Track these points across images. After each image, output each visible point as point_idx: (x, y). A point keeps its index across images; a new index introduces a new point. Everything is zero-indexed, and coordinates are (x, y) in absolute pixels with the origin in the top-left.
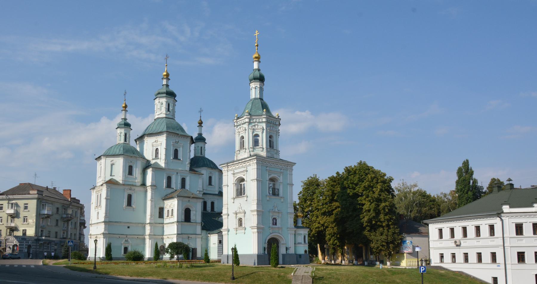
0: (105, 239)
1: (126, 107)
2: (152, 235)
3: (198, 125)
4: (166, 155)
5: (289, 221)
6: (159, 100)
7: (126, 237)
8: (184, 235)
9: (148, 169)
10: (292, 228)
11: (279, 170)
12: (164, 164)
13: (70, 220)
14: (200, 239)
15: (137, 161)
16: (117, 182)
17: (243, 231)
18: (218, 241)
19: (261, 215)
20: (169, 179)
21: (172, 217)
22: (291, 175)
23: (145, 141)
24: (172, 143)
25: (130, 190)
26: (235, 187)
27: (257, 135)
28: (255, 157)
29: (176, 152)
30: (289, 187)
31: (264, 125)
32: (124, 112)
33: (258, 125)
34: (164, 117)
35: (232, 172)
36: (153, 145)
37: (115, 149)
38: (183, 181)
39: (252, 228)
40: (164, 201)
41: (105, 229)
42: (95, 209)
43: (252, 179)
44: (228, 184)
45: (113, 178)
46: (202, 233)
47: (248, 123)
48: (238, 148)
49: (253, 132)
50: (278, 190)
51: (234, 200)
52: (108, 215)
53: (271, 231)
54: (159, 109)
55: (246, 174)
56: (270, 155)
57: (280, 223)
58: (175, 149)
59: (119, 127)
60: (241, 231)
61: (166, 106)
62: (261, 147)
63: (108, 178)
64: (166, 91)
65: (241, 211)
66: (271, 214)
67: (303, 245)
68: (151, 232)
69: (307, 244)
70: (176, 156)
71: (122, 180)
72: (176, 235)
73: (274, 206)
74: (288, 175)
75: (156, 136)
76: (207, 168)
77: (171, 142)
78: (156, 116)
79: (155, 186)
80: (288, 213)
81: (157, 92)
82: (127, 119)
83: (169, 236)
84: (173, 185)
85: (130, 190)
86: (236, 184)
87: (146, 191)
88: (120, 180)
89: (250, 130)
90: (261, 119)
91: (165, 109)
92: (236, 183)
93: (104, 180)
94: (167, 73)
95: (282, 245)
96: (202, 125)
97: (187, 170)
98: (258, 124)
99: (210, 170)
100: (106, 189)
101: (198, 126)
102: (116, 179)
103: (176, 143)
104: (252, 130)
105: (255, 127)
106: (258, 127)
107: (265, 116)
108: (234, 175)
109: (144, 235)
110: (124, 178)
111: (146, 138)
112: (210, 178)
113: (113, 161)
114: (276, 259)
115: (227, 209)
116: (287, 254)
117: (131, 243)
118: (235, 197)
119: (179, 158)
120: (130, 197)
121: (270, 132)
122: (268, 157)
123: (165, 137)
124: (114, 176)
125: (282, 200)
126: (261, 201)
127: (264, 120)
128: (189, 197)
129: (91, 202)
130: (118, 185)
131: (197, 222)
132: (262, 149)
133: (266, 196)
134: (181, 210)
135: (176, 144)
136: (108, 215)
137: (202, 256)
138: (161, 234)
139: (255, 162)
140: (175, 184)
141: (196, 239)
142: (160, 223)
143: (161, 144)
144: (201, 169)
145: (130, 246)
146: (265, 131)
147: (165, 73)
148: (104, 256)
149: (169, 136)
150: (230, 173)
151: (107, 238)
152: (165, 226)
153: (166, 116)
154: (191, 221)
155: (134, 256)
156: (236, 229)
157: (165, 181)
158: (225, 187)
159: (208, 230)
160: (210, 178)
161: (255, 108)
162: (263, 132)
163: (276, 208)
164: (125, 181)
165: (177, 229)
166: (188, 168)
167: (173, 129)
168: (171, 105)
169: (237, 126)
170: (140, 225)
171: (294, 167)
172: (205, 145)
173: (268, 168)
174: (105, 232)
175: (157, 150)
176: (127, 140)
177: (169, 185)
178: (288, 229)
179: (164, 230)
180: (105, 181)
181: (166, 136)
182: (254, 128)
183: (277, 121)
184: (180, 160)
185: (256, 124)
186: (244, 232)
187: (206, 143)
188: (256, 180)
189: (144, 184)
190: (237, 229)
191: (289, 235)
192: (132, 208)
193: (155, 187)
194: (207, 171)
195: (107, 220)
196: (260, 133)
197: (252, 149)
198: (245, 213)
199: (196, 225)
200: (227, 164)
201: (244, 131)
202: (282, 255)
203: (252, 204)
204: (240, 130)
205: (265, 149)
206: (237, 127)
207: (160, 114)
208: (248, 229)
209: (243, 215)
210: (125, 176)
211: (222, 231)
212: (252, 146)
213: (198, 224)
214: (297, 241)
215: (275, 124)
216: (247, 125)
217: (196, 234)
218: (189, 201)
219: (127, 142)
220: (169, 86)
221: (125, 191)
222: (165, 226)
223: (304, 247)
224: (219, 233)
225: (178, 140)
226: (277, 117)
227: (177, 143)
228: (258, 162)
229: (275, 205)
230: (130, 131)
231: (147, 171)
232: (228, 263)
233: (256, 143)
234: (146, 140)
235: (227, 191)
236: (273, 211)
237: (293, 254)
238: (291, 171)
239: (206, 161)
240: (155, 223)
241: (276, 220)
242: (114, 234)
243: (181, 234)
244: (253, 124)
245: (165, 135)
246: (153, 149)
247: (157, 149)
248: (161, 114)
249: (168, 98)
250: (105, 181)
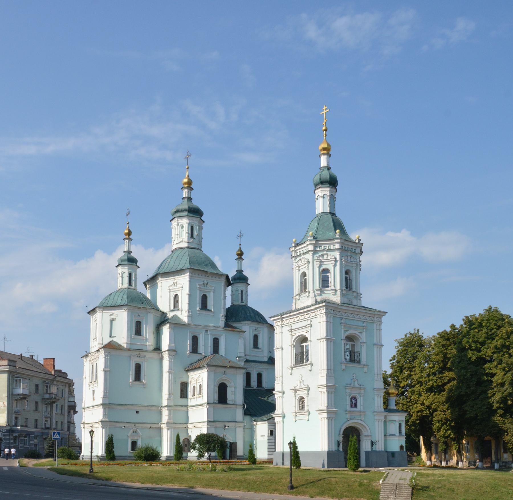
0: (104, 430)
1: (129, 233)
2: (172, 423)
3: (237, 257)
4: (189, 304)
5: (376, 402)
6: (179, 222)
7: (135, 425)
8: (217, 423)
9: (163, 325)
10: (381, 412)
11: (361, 324)
12: (187, 317)
13: (54, 402)
14: (242, 429)
15: (147, 314)
16: (120, 345)
17: (306, 417)
18: (268, 431)
19: (333, 392)
20: (195, 340)
21: (199, 397)
22: (379, 330)
23: (158, 283)
24: (198, 286)
25: (138, 357)
26: (293, 350)
27: (326, 271)
28: (324, 304)
29: (204, 299)
30: (375, 349)
31: (337, 255)
32: (127, 241)
33: (328, 255)
34: (186, 247)
35: (289, 328)
36: (170, 290)
37: (116, 297)
38: (216, 342)
39: (320, 411)
40: (188, 373)
41: (104, 415)
42: (89, 386)
43: (319, 337)
44: (283, 347)
45: (114, 339)
46: (244, 420)
47: (312, 252)
48: (298, 290)
49: (320, 266)
50: (360, 353)
51: (292, 370)
52: (108, 394)
53: (348, 416)
54: (178, 235)
55: (309, 331)
56: (346, 300)
57: (362, 404)
58: (203, 295)
59: (121, 264)
60: (303, 417)
61: (188, 230)
62: (333, 288)
63: (107, 340)
64: (189, 207)
65: (303, 386)
66: (348, 391)
67: (397, 438)
68: (169, 419)
69: (403, 436)
70: (204, 306)
71: (127, 343)
72: (206, 424)
73: (354, 379)
74: (375, 330)
75: (175, 276)
76: (250, 322)
77: (197, 284)
78: (174, 245)
79: (174, 351)
80: (375, 389)
81: (174, 210)
82: (132, 252)
83: (196, 425)
84: (201, 349)
85: (138, 357)
86: (294, 346)
87: (162, 359)
88: (123, 343)
89: (315, 263)
90: (332, 246)
91: (187, 235)
92: (295, 344)
93: (101, 343)
94: (189, 179)
95: (365, 438)
96: (242, 257)
97: (221, 326)
98: (328, 253)
99: (256, 326)
100: (104, 356)
101: (236, 260)
102: (117, 342)
103: (204, 286)
104: (319, 263)
105: (323, 258)
106: (327, 258)
107: (339, 241)
108: (292, 332)
109: (159, 423)
110: (129, 339)
111: (160, 279)
112: (256, 337)
113: (112, 314)
114: (356, 459)
115: (281, 384)
116: (372, 451)
117: (141, 434)
118: (294, 365)
119: (208, 308)
120: (138, 368)
121: (346, 265)
122: (343, 304)
123: (188, 277)
124: (115, 337)
125: (365, 369)
126: (332, 371)
127: (337, 246)
128: (225, 367)
129: (83, 375)
130: (121, 350)
131: (237, 404)
132: (334, 291)
133: (341, 363)
134: (212, 387)
135: (203, 288)
136: (108, 394)
137: (244, 454)
138: (184, 422)
139: (324, 311)
140: (203, 347)
141: (236, 428)
142: (182, 406)
143: (182, 287)
144: (241, 324)
145: (140, 439)
146: (338, 264)
147: (186, 180)
148: (103, 454)
149: (194, 275)
150: (286, 329)
151: (108, 428)
152: (190, 409)
153: (188, 245)
154: (228, 402)
155: (146, 454)
156: (295, 414)
157: (188, 344)
158: (278, 350)
159: (253, 415)
160: (256, 337)
161: (323, 229)
162: (335, 265)
163: (356, 383)
164: (131, 344)
165: (208, 413)
166: (222, 322)
167: (200, 264)
168: (196, 228)
169: (296, 257)
170: (153, 408)
171: (384, 319)
172: (247, 288)
173: (343, 321)
174: (104, 419)
175: (177, 296)
176: (133, 283)
177: (194, 349)
178: (375, 414)
179: (189, 415)
180: (102, 344)
181: (189, 276)
182: (322, 259)
183: (357, 247)
184: (210, 310)
185: (325, 252)
186: (307, 418)
187: (249, 285)
188: (325, 340)
189: (158, 349)
190: (296, 413)
191: (377, 423)
192: (142, 383)
193: (175, 353)
194: (250, 326)
195: (107, 402)
196: (331, 267)
197: (319, 292)
198: (309, 390)
199: (236, 407)
200: (281, 316)
201: (307, 265)
202: (365, 453)
203: (320, 375)
204: (300, 263)
205: (339, 291)
206: (296, 259)
207: (180, 243)
208: (314, 414)
209: (306, 392)
210: (131, 336)
211: (274, 417)
212: (319, 287)
213: (237, 406)
214: (388, 432)
215: (355, 252)
216: (311, 255)
217: (236, 422)
218: (225, 372)
219: (133, 287)
220: (192, 199)
221: (131, 359)
222: (189, 410)
223: (399, 440)
224: (269, 419)
225: (207, 281)
226: (357, 241)
227: (205, 285)
228: (329, 312)
229: (355, 378)
230: (136, 269)
231: (163, 329)
232: (283, 464)
233: (325, 282)
234: (160, 282)
235: (280, 356)
236: (352, 385)
237: (382, 451)
238: (378, 324)
239: (249, 311)
240: (177, 406)
241: (356, 400)
242: (116, 422)
243: (214, 421)
244: (321, 253)
245: (188, 274)
246: (170, 296)
247: (176, 296)
248: (181, 242)
249: (191, 218)
250: (102, 344)
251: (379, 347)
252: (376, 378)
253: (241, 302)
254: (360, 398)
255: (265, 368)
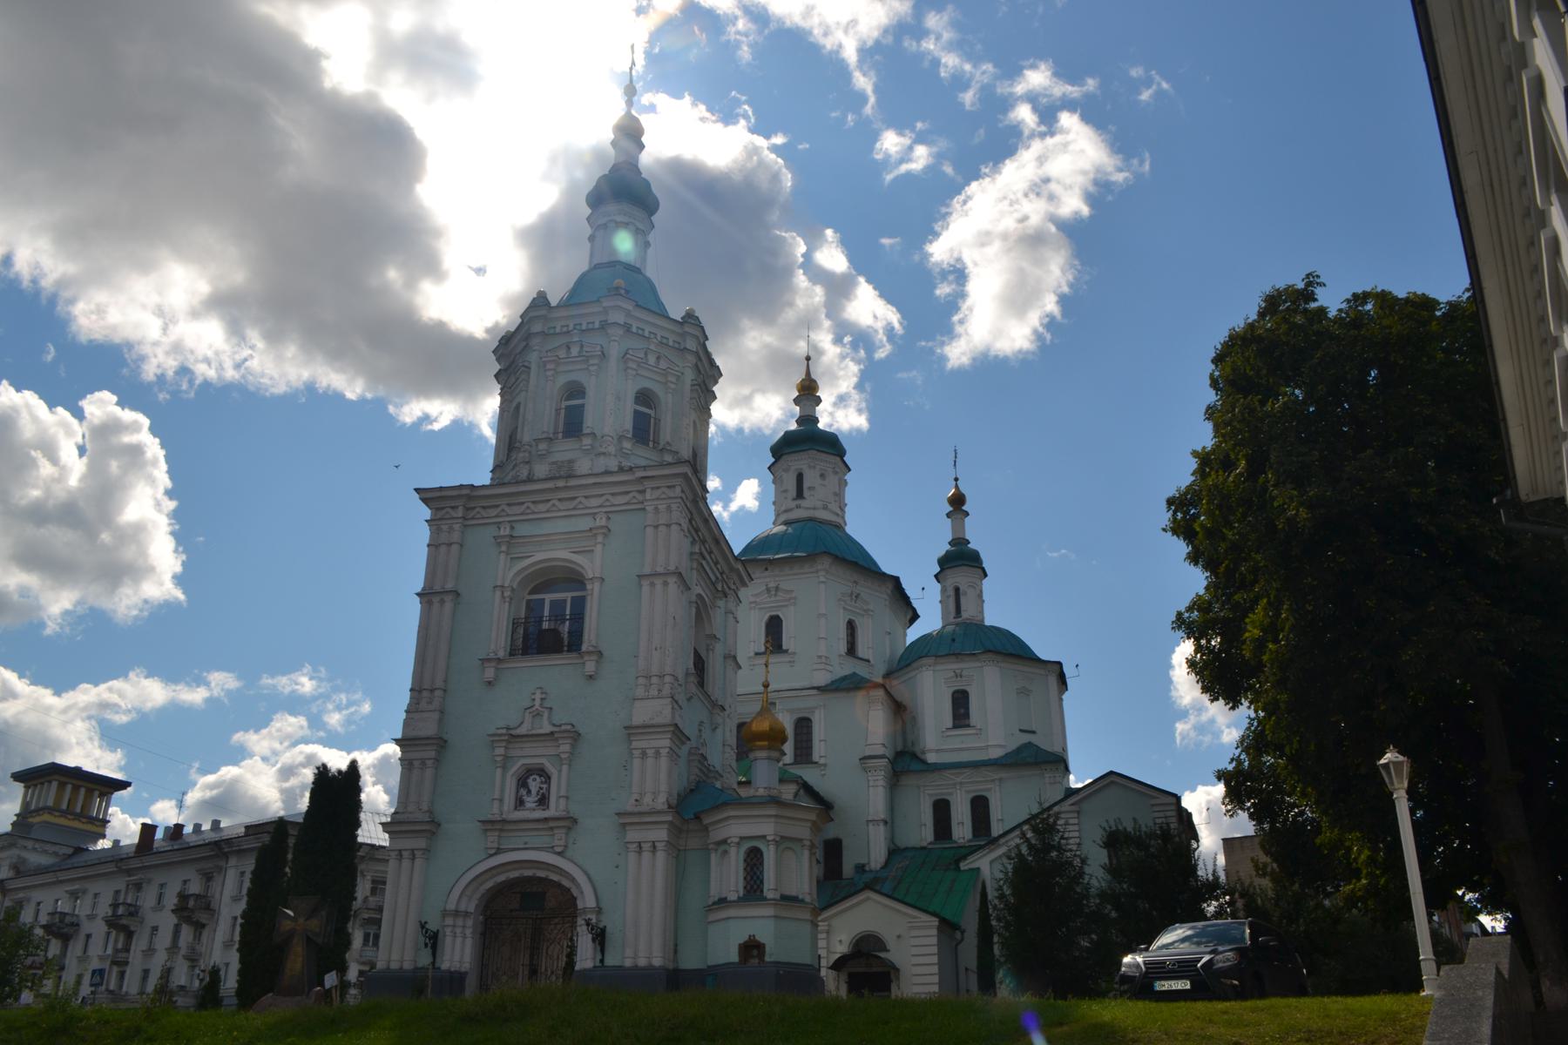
30: (646, 588)
96: (964, 508)
99: (954, 666)
125: (590, 667)
191: (632, 857)
214: (712, 893)
237: (650, 968)
238: (662, 507)
251: (658, 582)
252: (640, 692)
253: (955, 618)
254: (560, 771)
255: (993, 781)
